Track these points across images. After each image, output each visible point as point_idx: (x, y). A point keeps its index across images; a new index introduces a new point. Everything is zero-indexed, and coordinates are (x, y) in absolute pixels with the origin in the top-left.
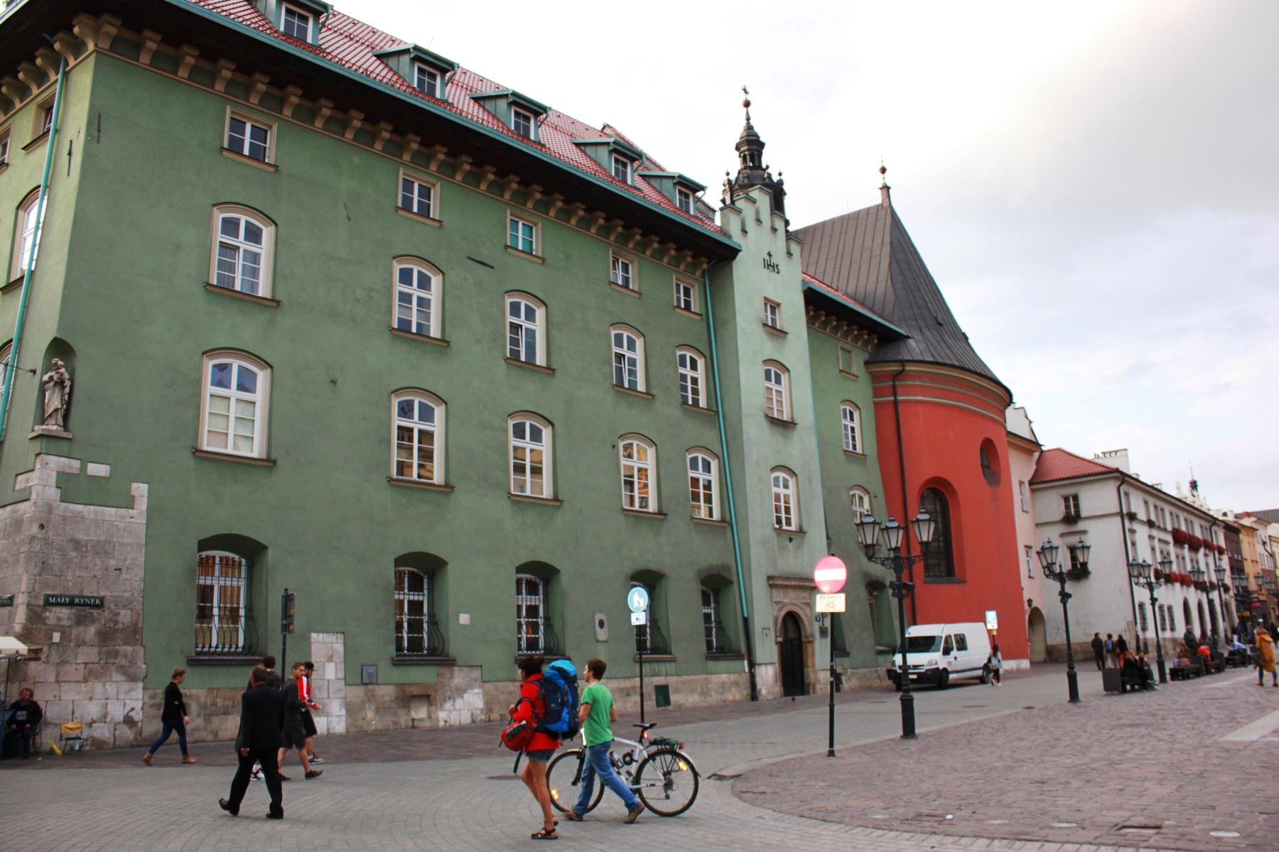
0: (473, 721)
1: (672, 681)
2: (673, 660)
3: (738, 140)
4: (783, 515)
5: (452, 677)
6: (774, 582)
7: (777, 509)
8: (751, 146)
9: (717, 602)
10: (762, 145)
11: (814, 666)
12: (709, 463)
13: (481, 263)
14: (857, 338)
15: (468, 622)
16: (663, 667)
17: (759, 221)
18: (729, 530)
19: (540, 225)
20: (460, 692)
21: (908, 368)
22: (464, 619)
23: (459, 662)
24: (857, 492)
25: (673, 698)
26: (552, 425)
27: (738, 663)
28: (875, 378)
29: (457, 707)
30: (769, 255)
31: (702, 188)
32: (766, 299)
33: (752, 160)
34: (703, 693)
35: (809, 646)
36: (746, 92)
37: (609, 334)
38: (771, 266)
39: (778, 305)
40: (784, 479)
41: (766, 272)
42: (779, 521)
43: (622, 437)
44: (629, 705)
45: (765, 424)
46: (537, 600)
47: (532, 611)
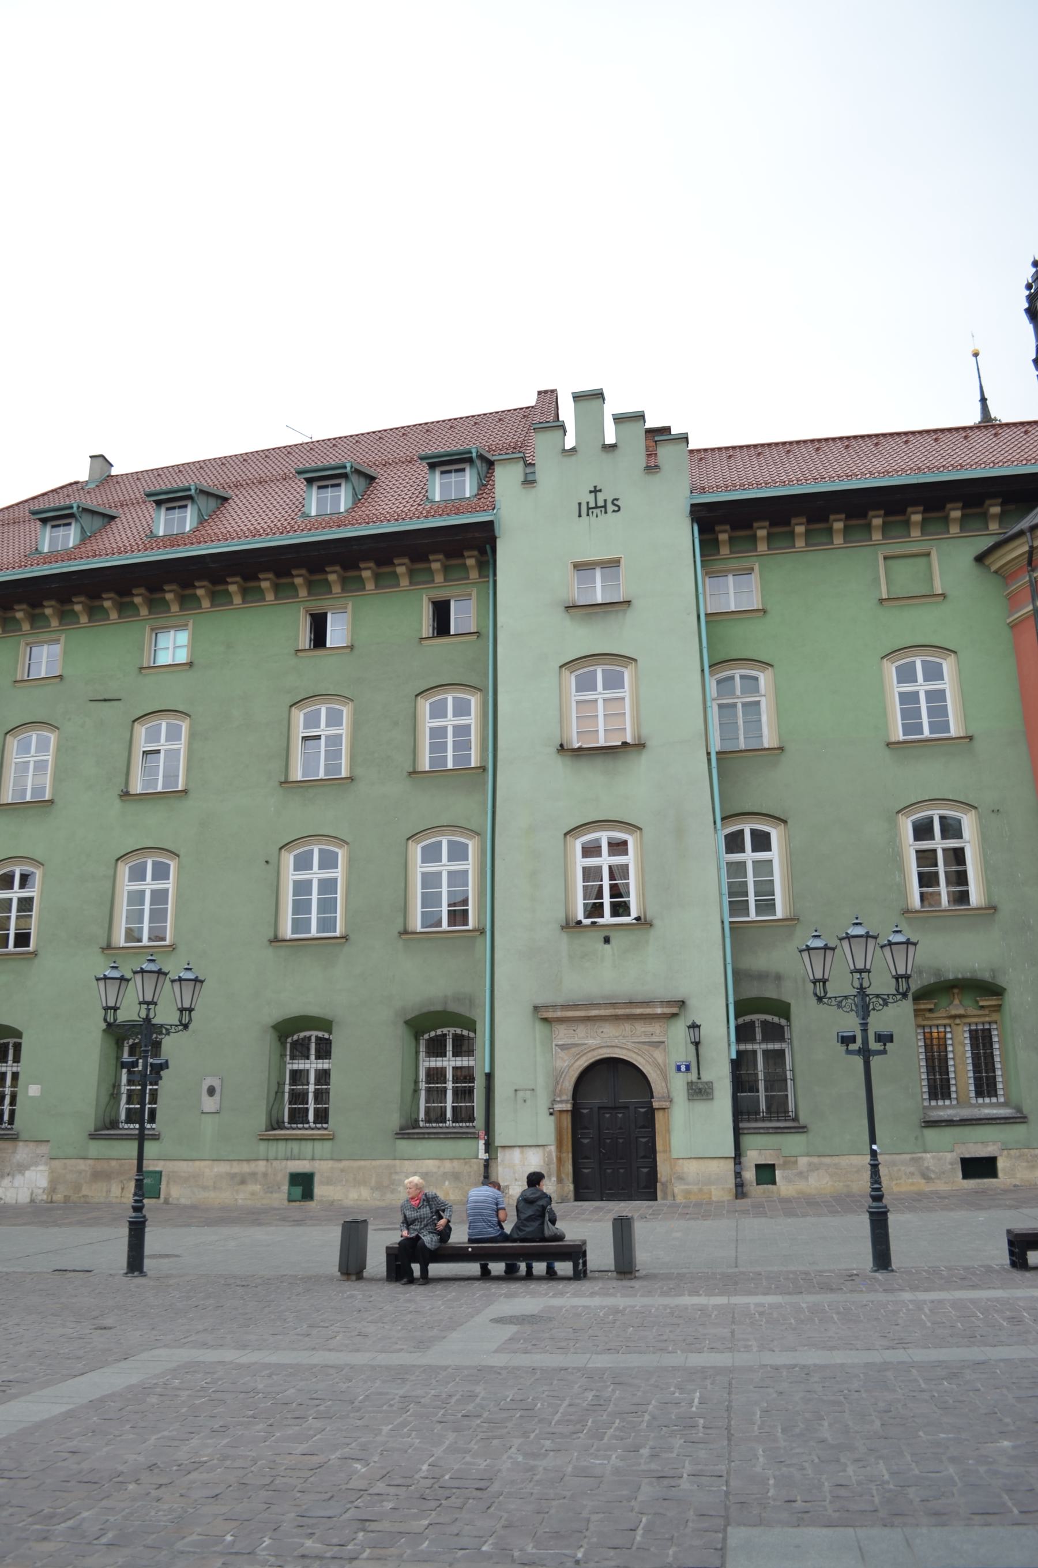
0: (32, 1201)
1: (321, 1168)
2: (331, 1139)
5: (14, 1152)
6: (546, 1016)
11: (668, 1150)
13: (105, 700)
16: (307, 1147)
20: (22, 1168)
23: (23, 1136)
25: (318, 1190)
26: (178, 856)
27: (463, 1146)
29: (16, 1184)
32: (578, 567)
34: (379, 1187)
35: (659, 1116)
44: (241, 1196)
45: (560, 766)
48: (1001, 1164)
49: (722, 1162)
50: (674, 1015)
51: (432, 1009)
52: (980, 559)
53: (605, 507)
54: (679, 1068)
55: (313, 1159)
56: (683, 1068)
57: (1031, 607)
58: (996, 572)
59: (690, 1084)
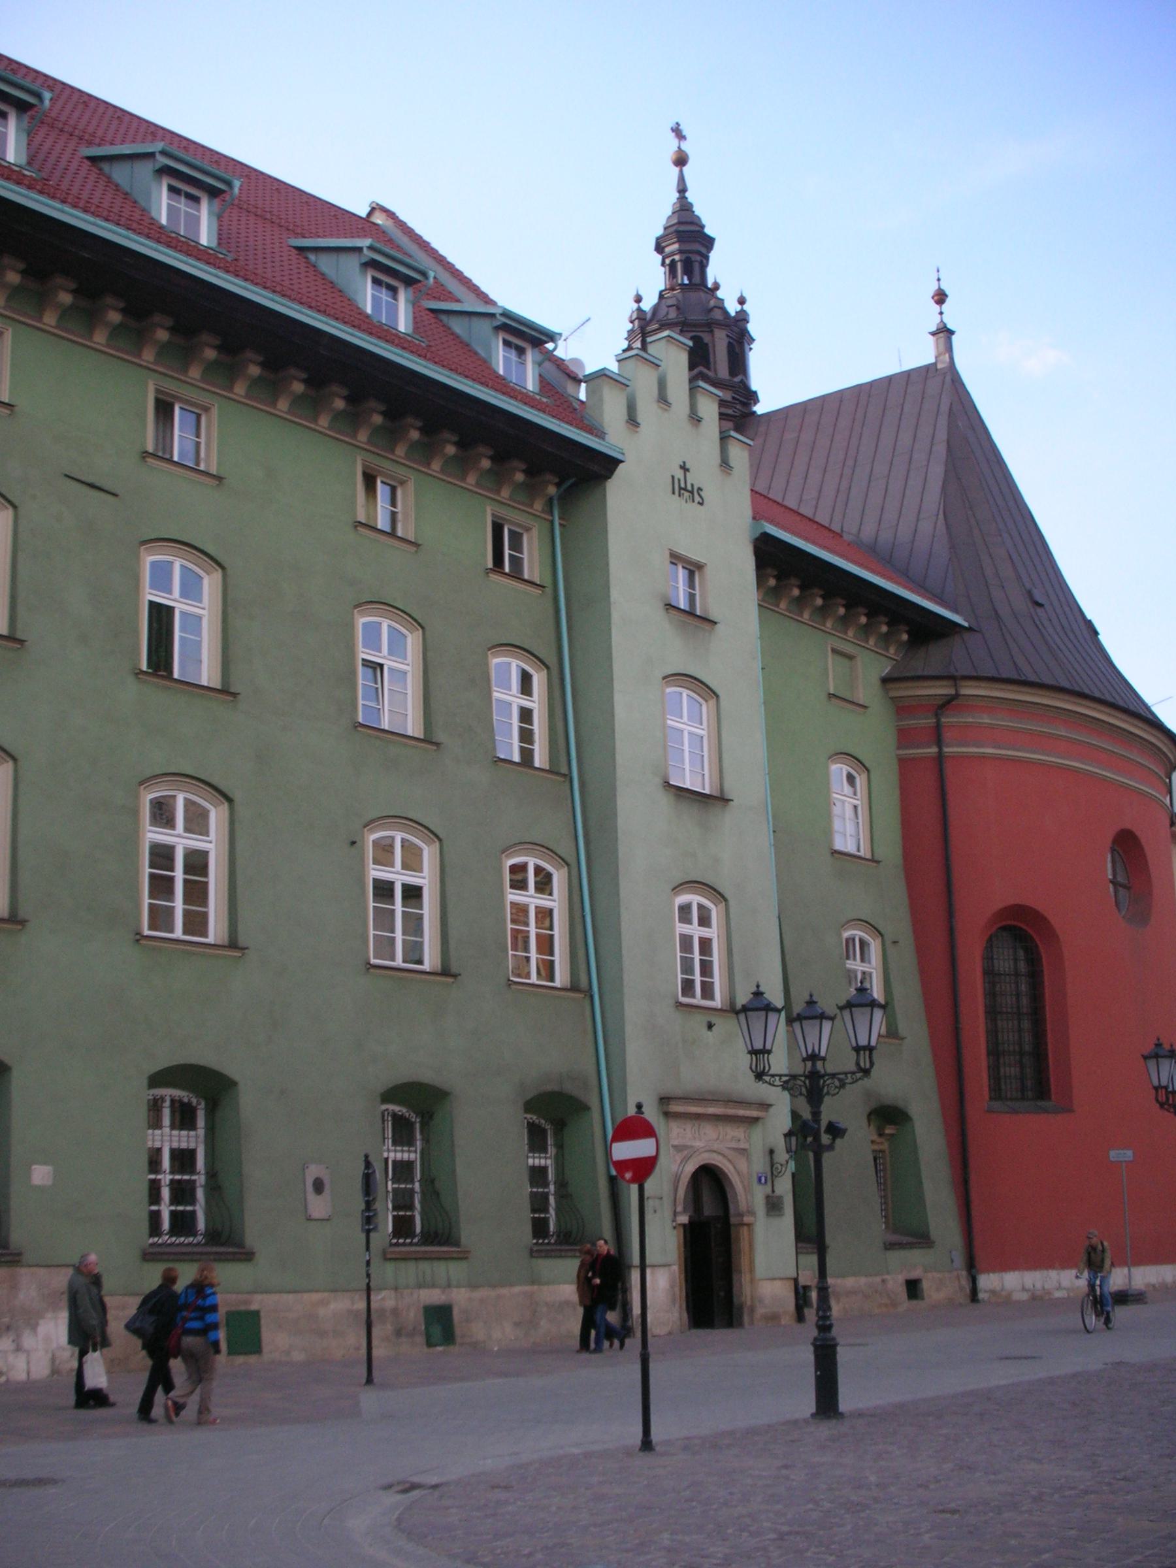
0: (55, 1371)
1: (460, 1298)
2: (464, 1256)
3: (660, 232)
4: (698, 978)
7: (687, 967)
8: (687, 243)
9: (560, 1146)
10: (709, 242)
11: (752, 1270)
12: (549, 876)
14: (867, 630)
15: (49, 1182)
17: (663, 399)
18: (587, 1002)
19: (215, 412)
21: (964, 691)
22: (41, 1174)
24: (858, 933)
26: (229, 800)
28: (902, 709)
30: (684, 468)
31: (552, 337)
33: (688, 271)
36: (678, 132)
37: (351, 626)
38: (686, 491)
39: (700, 567)
40: (701, 907)
41: (676, 502)
42: (688, 986)
43: (370, 824)
45: (665, 801)
46: (194, 1140)
47: (183, 1159)
48: (925, 1285)
49: (778, 1284)
50: (756, 1120)
51: (549, 1088)
52: (885, 681)
53: (692, 492)
54: (760, 1179)
55: (449, 1286)
56: (763, 1180)
57: (934, 750)
58: (891, 698)
59: (768, 1197)
